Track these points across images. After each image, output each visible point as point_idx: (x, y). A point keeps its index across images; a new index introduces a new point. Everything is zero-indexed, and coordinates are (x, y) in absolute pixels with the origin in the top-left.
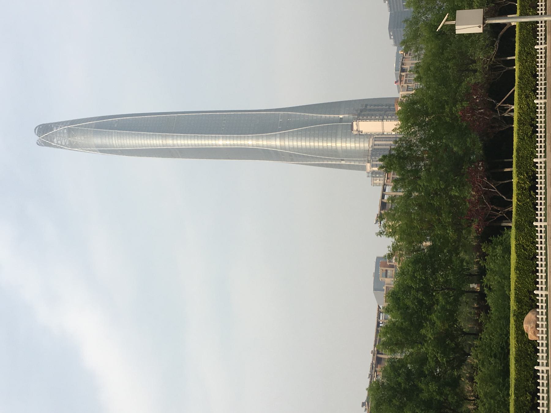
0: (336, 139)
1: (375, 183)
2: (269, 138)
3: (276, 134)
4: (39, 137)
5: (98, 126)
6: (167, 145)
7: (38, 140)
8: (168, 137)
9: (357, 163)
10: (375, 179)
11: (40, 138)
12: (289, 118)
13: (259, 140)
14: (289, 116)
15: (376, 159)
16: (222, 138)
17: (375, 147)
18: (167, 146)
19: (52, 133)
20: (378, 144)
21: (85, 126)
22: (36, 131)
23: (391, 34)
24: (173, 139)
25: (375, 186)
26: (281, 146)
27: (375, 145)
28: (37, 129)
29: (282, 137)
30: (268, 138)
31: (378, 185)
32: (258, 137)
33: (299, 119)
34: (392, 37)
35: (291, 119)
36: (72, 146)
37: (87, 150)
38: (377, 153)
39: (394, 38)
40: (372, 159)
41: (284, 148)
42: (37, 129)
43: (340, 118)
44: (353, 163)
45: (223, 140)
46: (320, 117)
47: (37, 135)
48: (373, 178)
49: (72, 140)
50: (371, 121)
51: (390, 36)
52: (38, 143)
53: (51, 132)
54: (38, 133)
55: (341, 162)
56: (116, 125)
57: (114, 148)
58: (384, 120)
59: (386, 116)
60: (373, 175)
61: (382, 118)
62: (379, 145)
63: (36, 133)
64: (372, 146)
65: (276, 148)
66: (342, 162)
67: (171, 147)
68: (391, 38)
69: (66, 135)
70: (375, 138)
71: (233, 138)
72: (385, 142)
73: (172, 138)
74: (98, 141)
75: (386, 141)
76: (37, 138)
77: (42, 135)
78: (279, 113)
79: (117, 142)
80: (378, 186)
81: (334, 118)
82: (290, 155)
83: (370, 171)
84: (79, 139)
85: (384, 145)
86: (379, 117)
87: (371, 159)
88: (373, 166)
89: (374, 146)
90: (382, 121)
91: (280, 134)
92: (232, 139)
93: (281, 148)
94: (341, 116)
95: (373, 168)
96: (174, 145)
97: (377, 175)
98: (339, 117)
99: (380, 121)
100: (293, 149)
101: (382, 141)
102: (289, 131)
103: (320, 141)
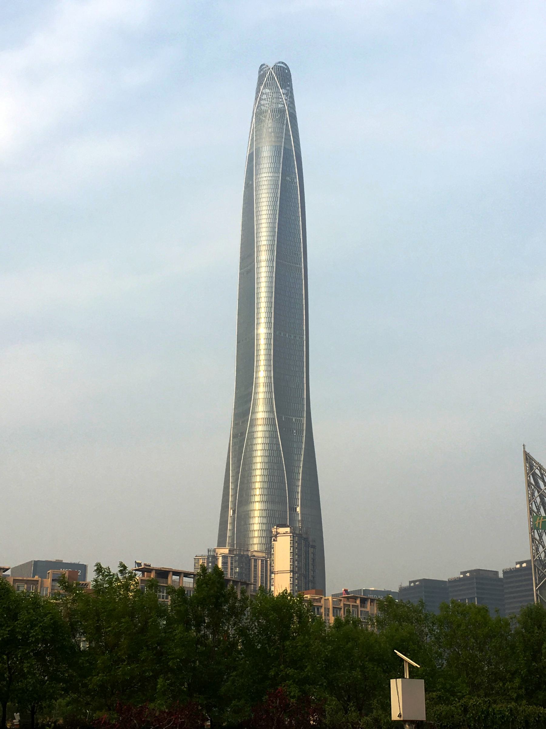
0: (266, 502)
1: (199, 561)
2: (267, 403)
3: (273, 412)
4: (272, 68)
5: (287, 152)
6: (258, 251)
7: (267, 66)
8: (269, 254)
9: (229, 534)
10: (206, 561)
11: (271, 69)
12: (296, 431)
13: (266, 387)
14: (300, 432)
15: (235, 562)
16: (269, 332)
17: (253, 560)
18: (257, 251)
19: (278, 87)
20: (257, 565)
21: (287, 135)
22: (281, 65)
23: (416, 583)
24: (269, 261)
25: (195, 561)
26: (254, 419)
27: (256, 560)
28: (284, 66)
29: (270, 422)
30: (269, 402)
31: (196, 565)
32: (270, 385)
33: (295, 446)
34: (412, 584)
35: (295, 434)
36: (259, 115)
37: (253, 135)
38: (244, 564)
39: (409, 588)
40: (235, 557)
41: (253, 425)
42: (284, 66)
43: (296, 508)
44: (229, 527)
45: (265, 333)
46: (298, 477)
47: (275, 66)
48: (207, 558)
49: (267, 114)
50: (291, 555)
51: (414, 582)
52: (264, 66)
53: (279, 86)
54: (278, 66)
55: (231, 509)
56: (288, 178)
57: (256, 175)
58: (292, 573)
59: (298, 577)
60: (210, 558)
61: (295, 570)
62: (255, 566)
63: (279, 65)
64: (254, 556)
65: (254, 412)
66: (232, 511)
67: (257, 258)
68: (410, 582)
69: (274, 106)
70: (266, 561)
71: (268, 349)
72: (260, 575)
73: (270, 259)
74: (266, 152)
75: (262, 577)
76: (271, 65)
77: (274, 73)
78: (303, 417)
79: (265, 179)
80: (195, 565)
81: (297, 499)
82: (243, 434)
83: (217, 554)
84: (269, 124)
85: (256, 574)
86: (296, 566)
87: (236, 555)
88: (225, 557)
89: (254, 559)
90: (290, 571)
91: (274, 419)
92: (267, 310)
93: (253, 420)
94: (298, 509)
95: (221, 557)
96: (259, 262)
97: (210, 564)
98: (298, 506)
99: (291, 567)
100: (252, 437)
101: (261, 571)
102: (277, 432)
103: (264, 440)
